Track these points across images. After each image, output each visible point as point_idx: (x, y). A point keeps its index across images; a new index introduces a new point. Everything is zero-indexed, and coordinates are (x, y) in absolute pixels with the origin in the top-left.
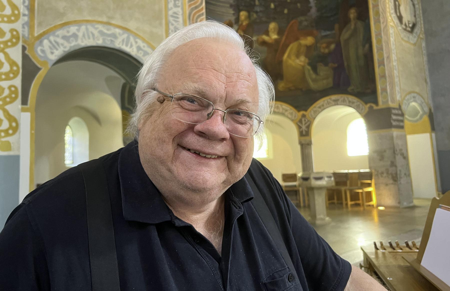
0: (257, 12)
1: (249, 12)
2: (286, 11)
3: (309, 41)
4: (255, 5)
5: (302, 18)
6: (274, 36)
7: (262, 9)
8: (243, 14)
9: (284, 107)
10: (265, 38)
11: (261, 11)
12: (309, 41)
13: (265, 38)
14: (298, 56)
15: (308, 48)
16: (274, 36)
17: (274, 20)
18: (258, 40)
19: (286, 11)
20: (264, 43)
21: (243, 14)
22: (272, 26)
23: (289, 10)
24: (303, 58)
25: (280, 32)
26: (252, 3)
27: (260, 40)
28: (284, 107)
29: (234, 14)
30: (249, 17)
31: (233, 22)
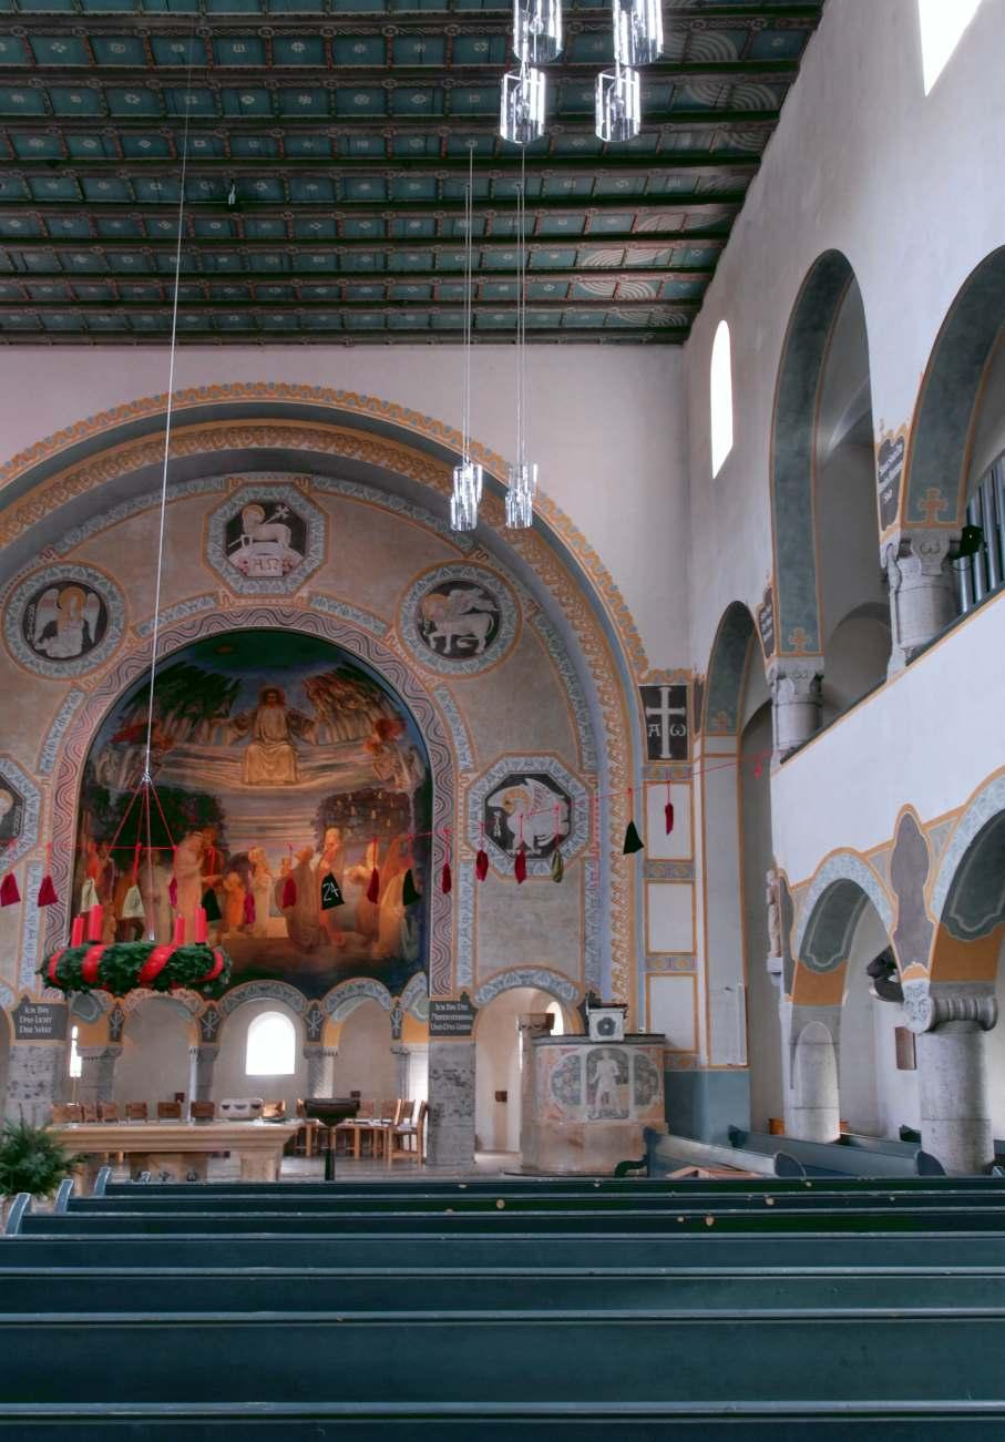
0: (352, 828)
1: (341, 828)
2: (389, 824)
4: (350, 816)
5: (403, 836)
7: (360, 822)
9: (379, 988)
11: (359, 825)
14: (396, 904)
18: (350, 875)
19: (389, 824)
23: (393, 821)
26: (346, 812)
27: (354, 874)
28: (379, 988)
29: (316, 836)
30: (341, 837)
31: (314, 848)
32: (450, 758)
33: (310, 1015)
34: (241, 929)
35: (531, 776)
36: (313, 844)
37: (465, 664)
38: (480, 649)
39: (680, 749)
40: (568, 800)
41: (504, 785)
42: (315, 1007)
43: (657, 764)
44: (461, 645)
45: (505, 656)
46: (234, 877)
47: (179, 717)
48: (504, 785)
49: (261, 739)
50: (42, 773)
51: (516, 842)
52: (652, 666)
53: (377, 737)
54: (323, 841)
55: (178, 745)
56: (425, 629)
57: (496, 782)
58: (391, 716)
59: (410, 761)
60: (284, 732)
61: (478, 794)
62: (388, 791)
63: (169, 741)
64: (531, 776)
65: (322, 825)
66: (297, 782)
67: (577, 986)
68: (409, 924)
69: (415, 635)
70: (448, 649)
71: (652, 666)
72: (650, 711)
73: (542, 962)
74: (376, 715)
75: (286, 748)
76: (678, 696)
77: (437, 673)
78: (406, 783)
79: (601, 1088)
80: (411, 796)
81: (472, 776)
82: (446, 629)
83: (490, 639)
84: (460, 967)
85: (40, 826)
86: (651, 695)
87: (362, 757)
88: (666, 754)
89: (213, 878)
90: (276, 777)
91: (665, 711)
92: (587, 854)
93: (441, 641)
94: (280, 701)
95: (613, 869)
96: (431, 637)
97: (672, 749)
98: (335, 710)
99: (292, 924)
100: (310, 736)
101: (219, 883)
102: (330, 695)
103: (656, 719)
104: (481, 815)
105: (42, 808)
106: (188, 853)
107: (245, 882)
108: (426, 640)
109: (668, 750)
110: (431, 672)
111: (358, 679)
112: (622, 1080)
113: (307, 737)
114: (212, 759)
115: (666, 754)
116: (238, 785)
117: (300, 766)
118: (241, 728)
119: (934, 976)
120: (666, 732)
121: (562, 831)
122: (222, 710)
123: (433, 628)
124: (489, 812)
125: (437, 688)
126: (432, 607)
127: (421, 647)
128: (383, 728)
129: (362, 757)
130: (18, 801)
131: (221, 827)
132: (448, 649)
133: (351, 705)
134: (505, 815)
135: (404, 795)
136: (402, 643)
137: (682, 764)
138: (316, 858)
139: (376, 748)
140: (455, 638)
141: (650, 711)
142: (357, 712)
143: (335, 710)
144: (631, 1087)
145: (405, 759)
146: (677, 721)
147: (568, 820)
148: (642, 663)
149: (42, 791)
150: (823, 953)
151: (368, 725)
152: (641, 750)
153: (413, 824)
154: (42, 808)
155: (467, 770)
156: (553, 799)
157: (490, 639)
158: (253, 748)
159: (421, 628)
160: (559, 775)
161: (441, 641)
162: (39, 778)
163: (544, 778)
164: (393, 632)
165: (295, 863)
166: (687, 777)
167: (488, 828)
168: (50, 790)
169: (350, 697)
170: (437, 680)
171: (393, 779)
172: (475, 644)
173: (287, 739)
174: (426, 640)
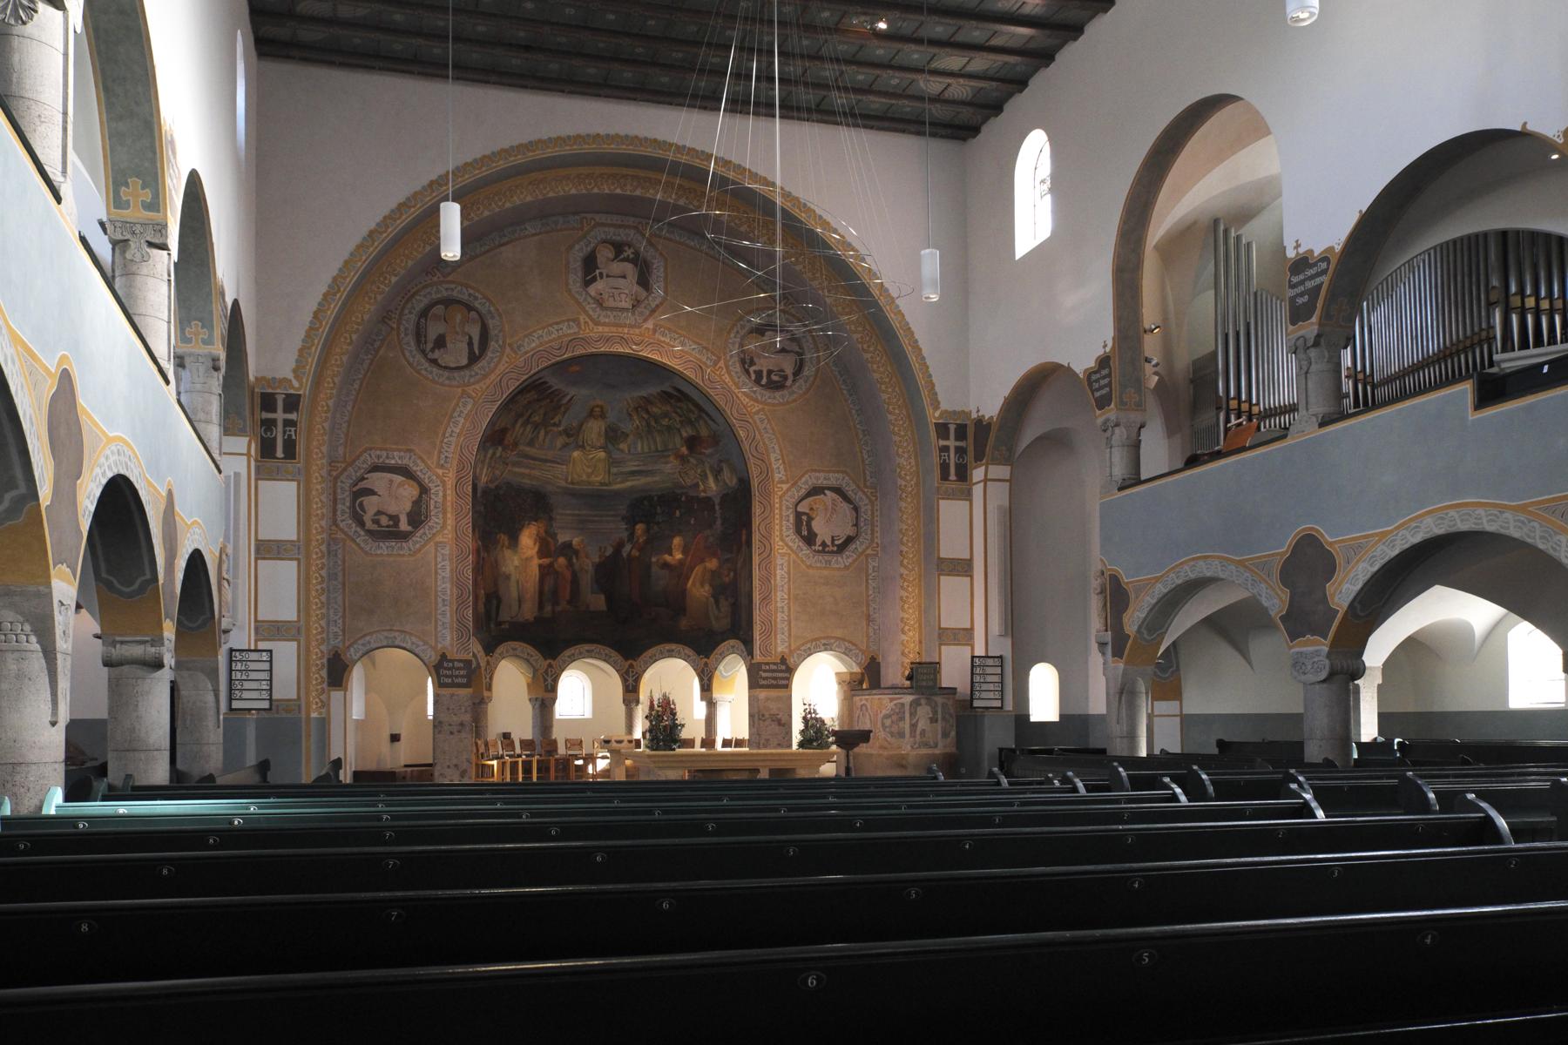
3: (712, 564)
5: (708, 532)
6: (679, 556)
8: (640, 528)
10: (667, 558)
12: (712, 564)
13: (667, 558)
14: (702, 585)
15: (713, 572)
16: (679, 556)
17: (679, 533)
20: (666, 565)
21: (640, 528)
22: (677, 541)
24: (707, 587)
25: (685, 551)
30: (648, 530)
32: (767, 473)
33: (627, 672)
34: (569, 602)
35: (829, 489)
36: (625, 535)
37: (778, 394)
38: (789, 383)
39: (963, 474)
40: (856, 509)
41: (808, 495)
42: (631, 666)
43: (946, 485)
44: (775, 378)
45: (808, 390)
46: (562, 560)
47: (525, 424)
48: (808, 495)
49: (583, 447)
50: (442, 467)
51: (819, 541)
52: (944, 406)
53: (684, 450)
54: (632, 535)
55: (521, 447)
56: (746, 362)
57: (803, 492)
58: (704, 432)
59: (717, 473)
60: (602, 440)
61: (789, 501)
62: (692, 493)
63: (516, 444)
64: (829, 489)
65: (631, 521)
66: (610, 484)
67: (863, 652)
68: (717, 602)
69: (738, 368)
70: (764, 381)
71: (944, 406)
72: (942, 443)
73: (839, 633)
74: (687, 432)
75: (602, 454)
76: (961, 432)
77: (756, 401)
78: (712, 487)
79: (920, 726)
80: (717, 501)
81: (785, 487)
82: (763, 364)
83: (798, 371)
84: (779, 636)
85: (445, 513)
86: (942, 430)
87: (670, 467)
88: (953, 477)
89: (546, 561)
90: (593, 478)
91: (952, 443)
92: (869, 551)
93: (759, 374)
94: (603, 416)
95: (902, 564)
96: (752, 370)
97: (957, 474)
98: (648, 425)
99: (609, 599)
100: (623, 446)
101: (551, 565)
102: (648, 412)
103: (945, 449)
104: (792, 518)
105: (445, 496)
106: (528, 539)
107: (570, 564)
108: (748, 372)
109: (957, 476)
110: (752, 399)
111: (679, 400)
112: (933, 720)
113: (622, 446)
114: (546, 461)
115: (953, 477)
116: (563, 484)
117: (614, 470)
118: (569, 436)
119: (1333, 645)
120: (953, 459)
121: (850, 531)
122: (556, 420)
123: (752, 363)
124: (798, 515)
125: (757, 412)
126: (752, 346)
127: (744, 378)
128: (693, 443)
129: (670, 467)
130: (424, 490)
131: (551, 519)
132: (764, 381)
133: (665, 422)
134: (810, 519)
135: (709, 499)
136: (729, 372)
137: (964, 486)
138: (628, 547)
139: (683, 459)
140: (770, 372)
141: (942, 443)
142: (669, 428)
143: (648, 425)
144: (939, 726)
145: (712, 468)
146: (961, 451)
147: (856, 525)
148: (936, 405)
149: (444, 482)
150: (1151, 630)
151: (678, 440)
152: (937, 473)
153: (719, 522)
154: (445, 496)
155: (782, 482)
156: (845, 505)
157: (798, 371)
158: (576, 454)
159: (743, 362)
160: (850, 489)
161: (759, 374)
162: (440, 472)
163: (838, 490)
164: (721, 364)
165: (609, 551)
166: (967, 496)
167: (798, 531)
168: (450, 483)
169: (666, 415)
170: (757, 407)
171: (697, 485)
172: (785, 378)
173: (604, 448)
174: (748, 372)
